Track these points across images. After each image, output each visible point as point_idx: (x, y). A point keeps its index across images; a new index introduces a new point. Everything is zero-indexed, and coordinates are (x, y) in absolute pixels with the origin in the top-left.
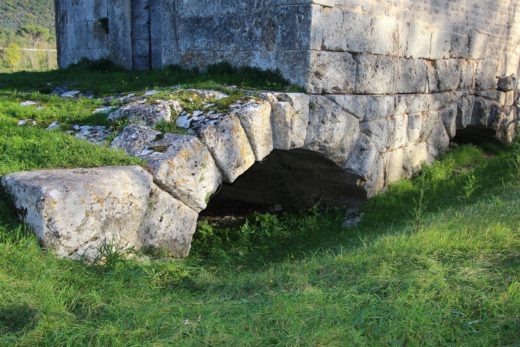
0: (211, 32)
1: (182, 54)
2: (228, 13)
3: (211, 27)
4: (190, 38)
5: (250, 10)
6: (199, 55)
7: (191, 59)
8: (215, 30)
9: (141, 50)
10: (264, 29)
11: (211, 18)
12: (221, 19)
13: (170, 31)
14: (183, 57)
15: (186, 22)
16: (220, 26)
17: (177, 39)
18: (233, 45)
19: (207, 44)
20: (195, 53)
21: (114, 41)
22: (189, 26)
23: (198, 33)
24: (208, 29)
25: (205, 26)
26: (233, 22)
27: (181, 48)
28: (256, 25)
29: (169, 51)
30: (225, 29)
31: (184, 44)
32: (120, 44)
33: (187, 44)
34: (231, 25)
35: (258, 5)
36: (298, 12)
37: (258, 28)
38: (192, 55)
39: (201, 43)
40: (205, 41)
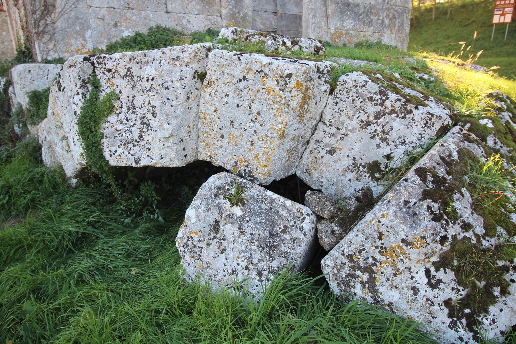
0: (357, 16)
1: (332, 32)
2: (370, 4)
3: (358, 12)
4: (340, 18)
5: (383, 5)
6: (347, 34)
7: (340, 37)
8: (361, 15)
9: (263, 24)
10: (390, 19)
11: (358, 5)
12: (365, 7)
13: (320, 8)
14: (333, 35)
15: (338, 3)
16: (364, 12)
17: (327, 17)
18: (372, 28)
19: (354, 25)
20: (344, 32)
21: (236, 8)
22: (340, 8)
23: (347, 15)
24: (355, 13)
25: (353, 10)
26: (373, 11)
27: (331, 26)
28: (386, 16)
29: (319, 28)
30: (367, 15)
31: (334, 24)
32: (245, 15)
33: (336, 24)
34: (371, 13)
35: (388, 3)
36: (406, 13)
37: (387, 19)
38: (341, 33)
39: (349, 24)
40: (352, 23)
